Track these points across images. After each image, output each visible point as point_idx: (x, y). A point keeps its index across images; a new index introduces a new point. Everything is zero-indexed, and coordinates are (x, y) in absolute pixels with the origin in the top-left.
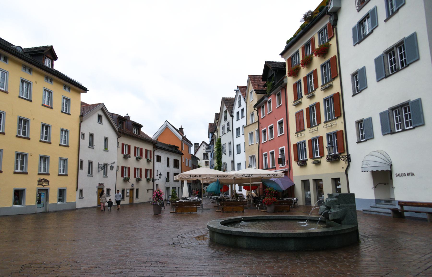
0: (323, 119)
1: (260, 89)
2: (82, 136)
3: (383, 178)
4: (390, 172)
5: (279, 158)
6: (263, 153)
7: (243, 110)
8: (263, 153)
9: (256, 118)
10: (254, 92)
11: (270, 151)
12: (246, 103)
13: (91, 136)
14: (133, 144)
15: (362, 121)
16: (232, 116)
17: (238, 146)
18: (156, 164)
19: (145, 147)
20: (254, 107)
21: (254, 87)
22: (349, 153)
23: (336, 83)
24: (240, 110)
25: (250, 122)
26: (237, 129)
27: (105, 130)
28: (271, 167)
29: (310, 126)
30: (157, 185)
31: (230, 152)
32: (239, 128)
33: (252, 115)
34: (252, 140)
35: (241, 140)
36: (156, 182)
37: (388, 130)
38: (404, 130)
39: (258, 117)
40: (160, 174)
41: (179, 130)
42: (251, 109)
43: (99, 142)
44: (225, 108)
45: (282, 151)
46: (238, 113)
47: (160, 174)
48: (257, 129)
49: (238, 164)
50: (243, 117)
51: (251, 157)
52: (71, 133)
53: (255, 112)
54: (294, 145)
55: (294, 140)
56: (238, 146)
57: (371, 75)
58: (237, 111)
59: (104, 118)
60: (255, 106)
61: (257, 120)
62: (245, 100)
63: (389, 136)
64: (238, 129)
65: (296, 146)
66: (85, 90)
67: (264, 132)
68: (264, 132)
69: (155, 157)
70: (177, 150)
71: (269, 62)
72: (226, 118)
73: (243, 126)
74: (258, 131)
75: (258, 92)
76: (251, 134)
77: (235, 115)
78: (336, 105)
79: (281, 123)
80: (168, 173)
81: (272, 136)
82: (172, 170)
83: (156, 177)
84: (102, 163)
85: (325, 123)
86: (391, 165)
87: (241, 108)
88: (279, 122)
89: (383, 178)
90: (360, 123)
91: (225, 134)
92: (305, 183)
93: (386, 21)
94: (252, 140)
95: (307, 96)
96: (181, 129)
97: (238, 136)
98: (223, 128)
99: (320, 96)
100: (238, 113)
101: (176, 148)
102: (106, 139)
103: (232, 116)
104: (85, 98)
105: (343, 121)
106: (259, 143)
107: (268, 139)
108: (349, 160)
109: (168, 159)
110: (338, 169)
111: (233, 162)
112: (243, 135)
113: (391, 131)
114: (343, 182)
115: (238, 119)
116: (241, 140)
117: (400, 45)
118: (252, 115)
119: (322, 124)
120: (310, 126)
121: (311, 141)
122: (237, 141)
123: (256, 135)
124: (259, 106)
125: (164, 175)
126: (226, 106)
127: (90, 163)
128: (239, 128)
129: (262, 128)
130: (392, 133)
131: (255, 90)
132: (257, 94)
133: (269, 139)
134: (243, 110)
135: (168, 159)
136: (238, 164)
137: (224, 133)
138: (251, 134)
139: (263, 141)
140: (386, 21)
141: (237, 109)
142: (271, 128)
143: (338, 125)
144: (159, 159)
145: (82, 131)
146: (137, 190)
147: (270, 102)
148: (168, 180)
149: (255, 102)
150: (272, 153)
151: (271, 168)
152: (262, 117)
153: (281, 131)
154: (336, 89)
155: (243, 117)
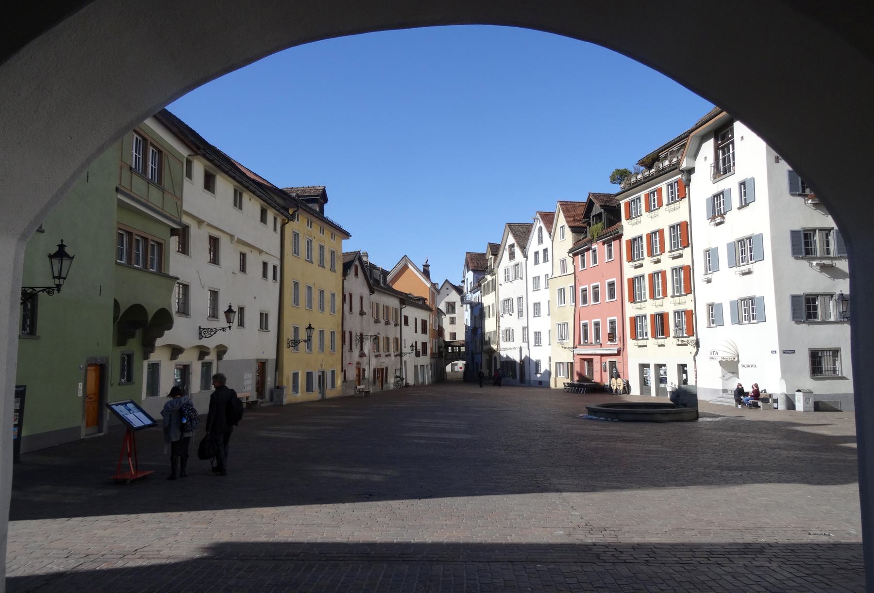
1: (578, 224)
3: (731, 366)
7: (545, 250)
9: (570, 269)
10: (568, 230)
11: (593, 321)
13: (351, 296)
15: (713, 304)
16: (526, 256)
17: (537, 306)
19: (394, 303)
20: (569, 253)
21: (567, 222)
23: (686, 252)
24: (540, 249)
26: (534, 278)
27: (357, 285)
29: (653, 296)
33: (563, 262)
34: (562, 299)
35: (543, 296)
36: (404, 358)
37: (737, 320)
38: (750, 323)
45: (612, 323)
46: (537, 253)
52: (336, 296)
53: (570, 260)
61: (573, 271)
64: (536, 279)
66: (347, 235)
67: (584, 290)
68: (584, 290)
70: (424, 303)
73: (547, 275)
74: (574, 288)
75: (575, 230)
76: (562, 291)
78: (685, 279)
82: (421, 338)
83: (404, 351)
87: (543, 247)
89: (731, 366)
90: (711, 306)
92: (644, 367)
93: (739, 209)
94: (562, 299)
96: (426, 266)
97: (536, 288)
98: (506, 271)
99: (667, 263)
100: (537, 253)
101: (424, 300)
102: (361, 298)
103: (526, 256)
108: (697, 344)
109: (416, 319)
110: (685, 354)
111: (525, 329)
114: (690, 369)
115: (536, 262)
116: (543, 296)
118: (563, 262)
119: (669, 298)
120: (653, 296)
122: (534, 297)
124: (575, 252)
126: (515, 237)
127: (351, 333)
129: (580, 285)
130: (739, 323)
131: (570, 227)
134: (545, 250)
135: (416, 319)
137: (507, 279)
138: (562, 291)
139: (580, 304)
140: (739, 209)
141: (533, 245)
143: (687, 303)
146: (387, 369)
149: (571, 246)
150: (597, 324)
153: (612, 296)
154: (685, 261)
155: (546, 260)
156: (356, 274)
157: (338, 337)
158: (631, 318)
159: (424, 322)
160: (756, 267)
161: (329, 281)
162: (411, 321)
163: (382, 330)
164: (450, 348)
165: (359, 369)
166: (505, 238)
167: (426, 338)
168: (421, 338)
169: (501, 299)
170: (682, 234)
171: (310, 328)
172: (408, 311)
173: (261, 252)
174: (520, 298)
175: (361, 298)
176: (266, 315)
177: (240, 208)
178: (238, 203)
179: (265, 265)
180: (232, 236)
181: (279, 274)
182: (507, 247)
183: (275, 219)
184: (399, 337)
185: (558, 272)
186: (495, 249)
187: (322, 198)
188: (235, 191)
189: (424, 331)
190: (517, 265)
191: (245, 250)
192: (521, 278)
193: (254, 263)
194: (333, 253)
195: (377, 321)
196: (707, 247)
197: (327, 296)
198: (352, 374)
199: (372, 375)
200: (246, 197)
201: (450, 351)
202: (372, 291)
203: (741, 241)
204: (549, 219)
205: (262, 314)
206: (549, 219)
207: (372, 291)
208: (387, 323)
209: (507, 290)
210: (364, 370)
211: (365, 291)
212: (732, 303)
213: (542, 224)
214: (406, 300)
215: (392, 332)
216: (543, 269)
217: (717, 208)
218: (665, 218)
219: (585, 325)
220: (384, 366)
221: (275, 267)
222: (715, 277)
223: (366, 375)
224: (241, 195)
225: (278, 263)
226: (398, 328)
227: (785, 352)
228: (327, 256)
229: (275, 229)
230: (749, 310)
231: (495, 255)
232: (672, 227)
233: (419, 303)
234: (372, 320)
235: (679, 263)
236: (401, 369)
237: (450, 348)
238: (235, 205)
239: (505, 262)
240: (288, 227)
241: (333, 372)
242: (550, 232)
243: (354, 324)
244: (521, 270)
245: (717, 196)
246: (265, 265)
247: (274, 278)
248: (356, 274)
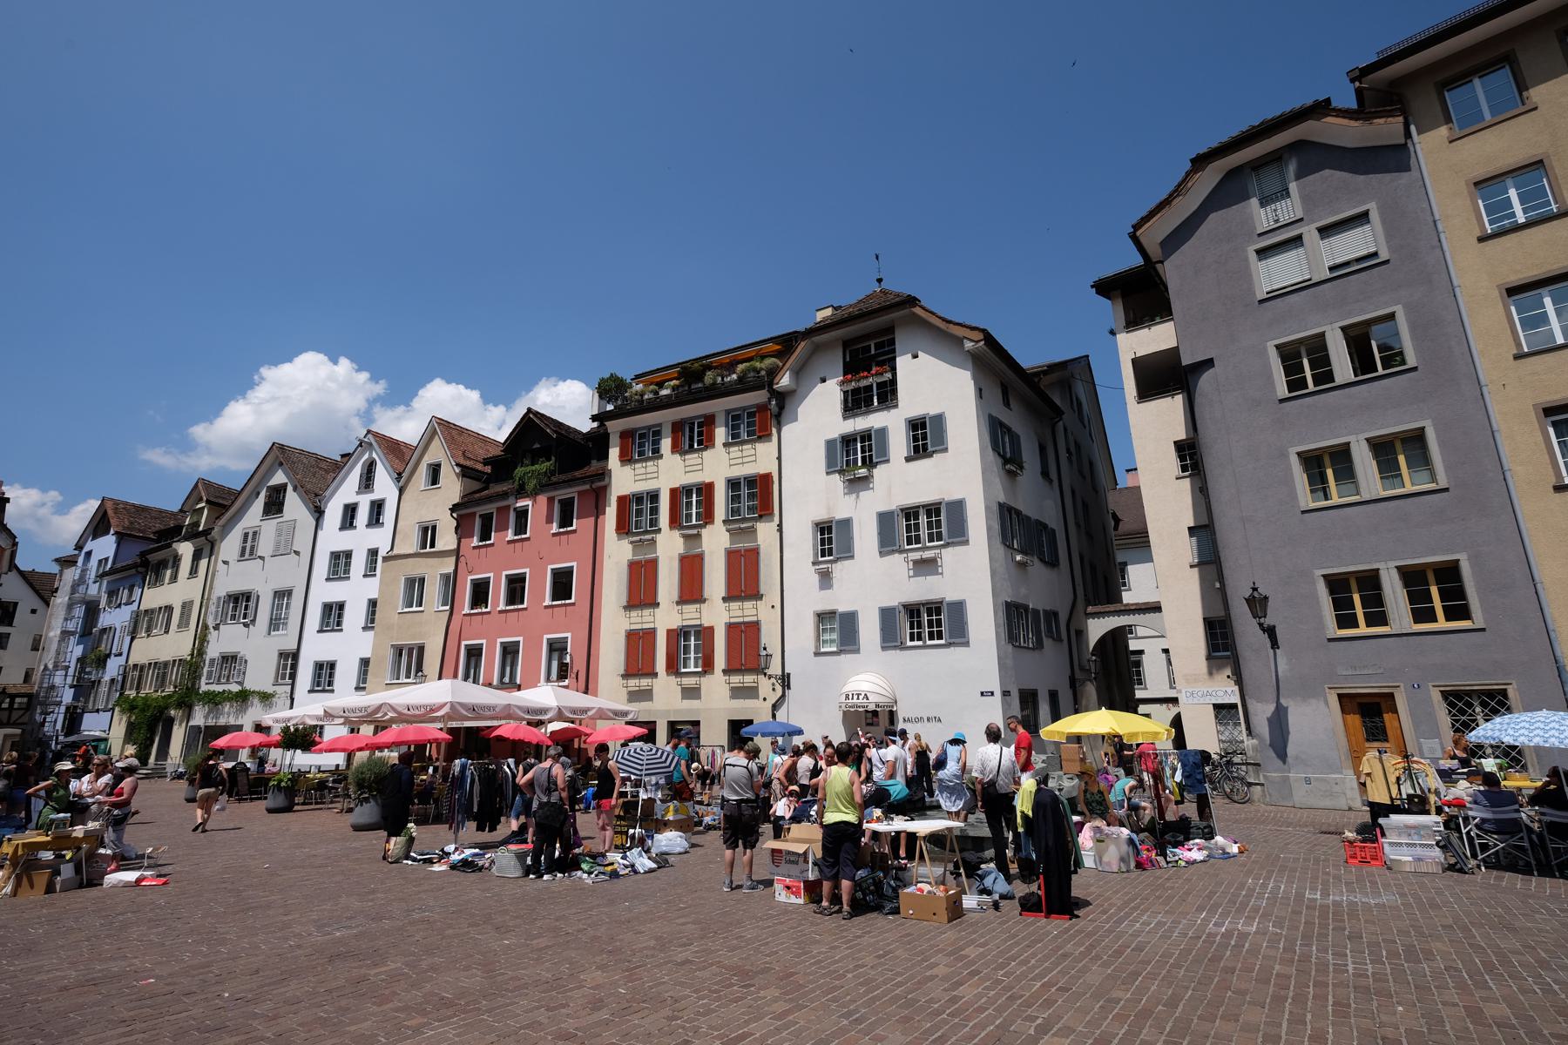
8: (464, 643)
12: (401, 491)
32: (348, 555)
48: (450, 569)
49: (319, 666)
57: (866, 536)
60: (454, 509)
71: (537, 414)
87: (376, 495)
91: (262, 558)
99: (716, 541)
100: (350, 511)
117: (933, 510)
123: (433, 591)
128: (348, 555)
130: (902, 647)
149: (457, 500)
160: (950, 557)
170: (757, 496)
174: (282, 595)
185: (410, 544)
196: (822, 515)
203: (910, 513)
217: (855, 457)
218: (718, 464)
222: (840, 570)
230: (927, 622)
232: (733, 484)
244: (302, 542)
245: (848, 441)
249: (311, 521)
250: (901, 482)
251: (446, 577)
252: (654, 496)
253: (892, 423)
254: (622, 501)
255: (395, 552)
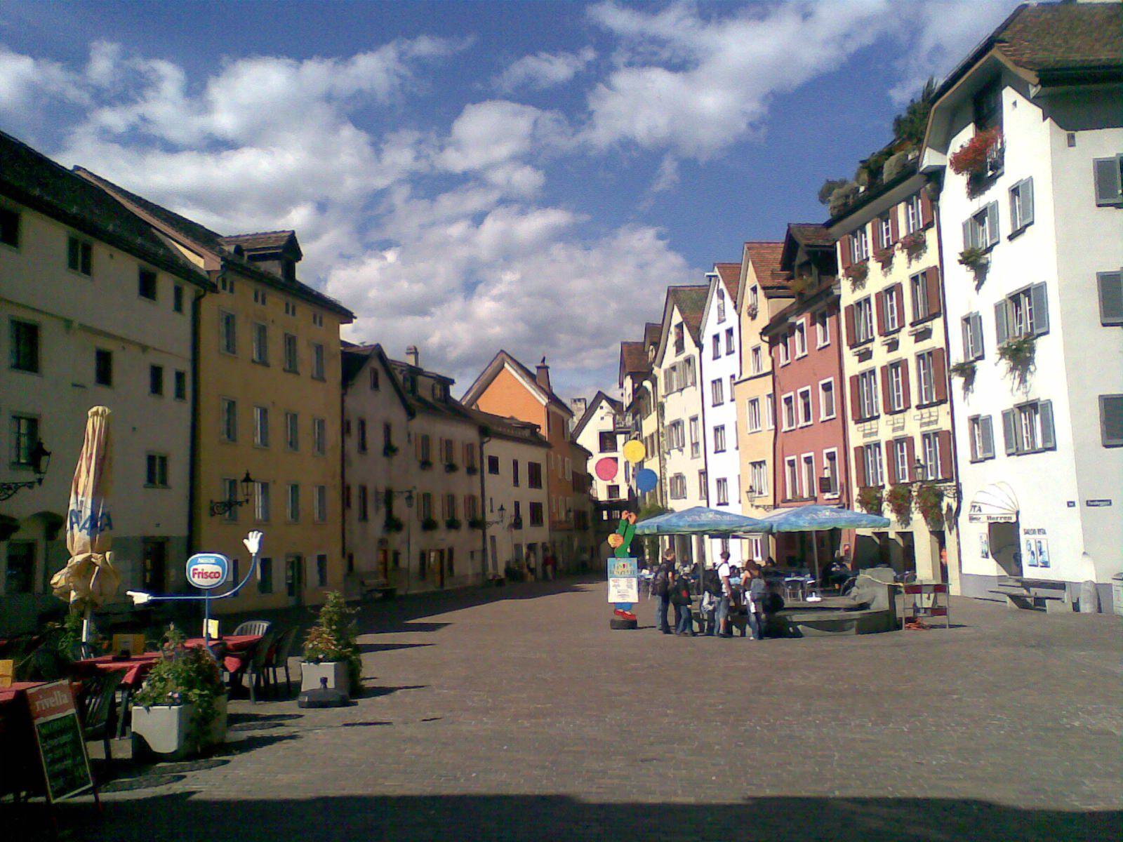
0: (914, 400)
2: (346, 428)
4: (1016, 524)
5: (822, 479)
6: (787, 459)
7: (730, 332)
9: (767, 367)
10: (760, 292)
11: (804, 456)
13: (362, 424)
14: (441, 429)
16: (699, 345)
18: (488, 477)
19: (464, 434)
22: (960, 481)
23: (937, 325)
25: (749, 371)
26: (714, 382)
28: (806, 495)
30: (493, 538)
31: (695, 445)
32: (720, 380)
36: (490, 531)
39: (773, 361)
40: (502, 509)
41: (534, 371)
42: (752, 335)
43: (375, 440)
44: (677, 318)
46: (716, 338)
47: (502, 509)
48: (770, 391)
49: (719, 481)
50: (730, 352)
51: (754, 464)
52: (328, 424)
54: (856, 449)
55: (857, 436)
56: (719, 429)
58: (715, 333)
59: (382, 376)
60: (764, 332)
62: (735, 307)
63: (1014, 458)
64: (717, 382)
65: (861, 451)
68: (788, 401)
69: (486, 461)
72: (680, 347)
73: (733, 377)
74: (773, 397)
77: (707, 341)
79: (827, 387)
80: (517, 505)
81: (807, 418)
82: (526, 495)
83: (489, 517)
84: (382, 489)
85: (919, 407)
86: (1017, 513)
88: (823, 385)
93: (1011, 238)
95: (883, 338)
96: (543, 368)
100: (716, 338)
101: (533, 428)
102: (387, 429)
103: (699, 345)
104: (347, 332)
105: (949, 410)
106: (776, 430)
107: (798, 423)
109: (516, 464)
111: (704, 473)
112: (732, 400)
113: (1017, 449)
115: (716, 357)
118: (756, 350)
120: (890, 411)
121: (893, 445)
122: (714, 417)
123: (765, 407)
124: (777, 332)
125: (510, 510)
127: (363, 489)
128: (720, 380)
129: (783, 392)
130: (1019, 453)
131: (764, 288)
132: (769, 297)
133: (802, 423)
134: (730, 332)
135: (516, 464)
136: (719, 481)
138: (754, 402)
139: (785, 428)
140: (1011, 238)
141: (711, 327)
142: (805, 395)
144: (494, 465)
145: (346, 418)
146: (451, 551)
147: (801, 329)
148: (517, 524)
149: (767, 322)
151: (806, 500)
152: (783, 362)
154: (936, 341)
155: (730, 352)
156: (375, 385)
157: (334, 496)
158: (856, 449)
159: (534, 470)
161: (316, 399)
162: (505, 466)
163: (435, 482)
164: (605, 513)
165: (385, 553)
166: (667, 314)
167: (539, 495)
168: (526, 495)
169: (667, 423)
171: (247, 479)
172: (494, 447)
173: (144, 348)
174: (694, 419)
175: (387, 429)
176: (164, 460)
177: (87, 269)
178: (80, 260)
179: (156, 373)
180: (68, 323)
181: (190, 385)
182: (672, 329)
183: (178, 292)
184: (478, 493)
186: (655, 334)
187: (289, 249)
188: (73, 243)
189: (535, 481)
190: (688, 361)
191: (107, 345)
192: (694, 384)
193: (130, 372)
194: (319, 349)
195: (426, 464)
196: (964, 313)
197: (305, 424)
198: (367, 560)
199: (415, 563)
200: (101, 253)
201: (605, 517)
202: (411, 414)
203: (1015, 298)
204: (733, 276)
205: (151, 459)
206: (733, 276)
207: (411, 414)
208: (451, 468)
209: (679, 406)
210: (396, 554)
211: (397, 415)
212: (1005, 415)
213: (722, 286)
214: (490, 427)
215: (462, 485)
216: (725, 367)
219: (792, 463)
220: (444, 546)
221: (180, 376)
223: (403, 563)
224: (87, 249)
225: (187, 368)
226: (477, 478)
227: (1090, 503)
228: (305, 354)
229: (178, 307)
230: (1029, 425)
231: (656, 344)
232: (914, 279)
233: (526, 435)
234: (415, 468)
235: (926, 345)
236: (484, 551)
237: (605, 513)
238: (73, 264)
239: (671, 357)
240: (208, 304)
241: (322, 560)
242: (734, 299)
243: (372, 471)
245: (979, 217)
246: (156, 373)
247: (180, 394)
248: (375, 385)
249: (697, 350)
250: (1013, 266)
251: (769, 396)
252: (867, 300)
253: (998, 193)
254: (850, 309)
255: (744, 377)
